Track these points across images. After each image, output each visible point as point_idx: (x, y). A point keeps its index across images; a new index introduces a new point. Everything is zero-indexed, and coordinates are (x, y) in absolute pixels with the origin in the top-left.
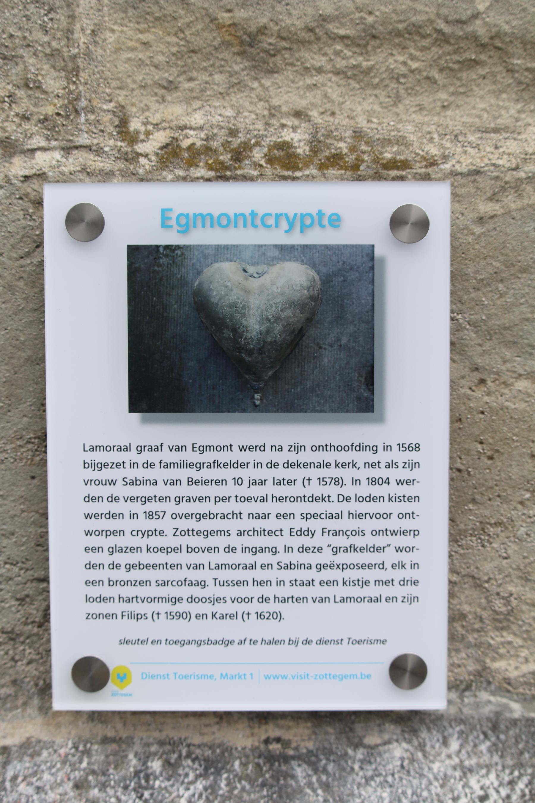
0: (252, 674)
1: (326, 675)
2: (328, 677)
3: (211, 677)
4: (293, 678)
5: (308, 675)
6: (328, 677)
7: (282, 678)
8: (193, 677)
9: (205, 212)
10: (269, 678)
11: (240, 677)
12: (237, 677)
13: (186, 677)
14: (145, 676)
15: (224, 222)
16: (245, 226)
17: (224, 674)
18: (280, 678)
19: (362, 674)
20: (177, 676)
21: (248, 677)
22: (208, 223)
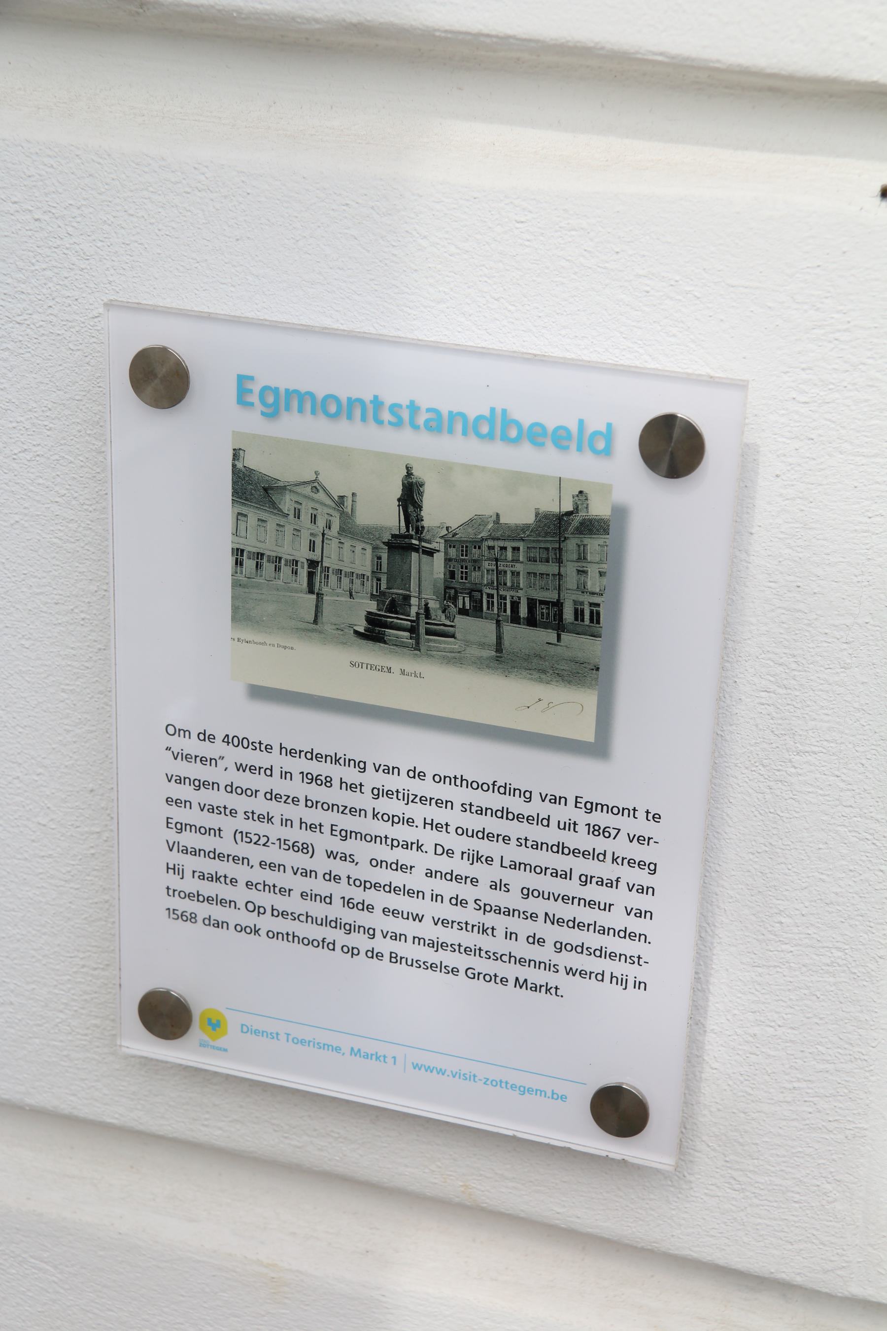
2: (504, 1085)
3: (337, 1049)
6: (504, 1085)
8: (311, 1044)
9: (303, 389)
10: (420, 1069)
11: (378, 1058)
13: (302, 1042)
14: (245, 1029)
15: (333, 409)
16: (364, 419)
17: (356, 1051)
19: (553, 1094)
20: (291, 1038)
21: (390, 1060)
22: (308, 406)
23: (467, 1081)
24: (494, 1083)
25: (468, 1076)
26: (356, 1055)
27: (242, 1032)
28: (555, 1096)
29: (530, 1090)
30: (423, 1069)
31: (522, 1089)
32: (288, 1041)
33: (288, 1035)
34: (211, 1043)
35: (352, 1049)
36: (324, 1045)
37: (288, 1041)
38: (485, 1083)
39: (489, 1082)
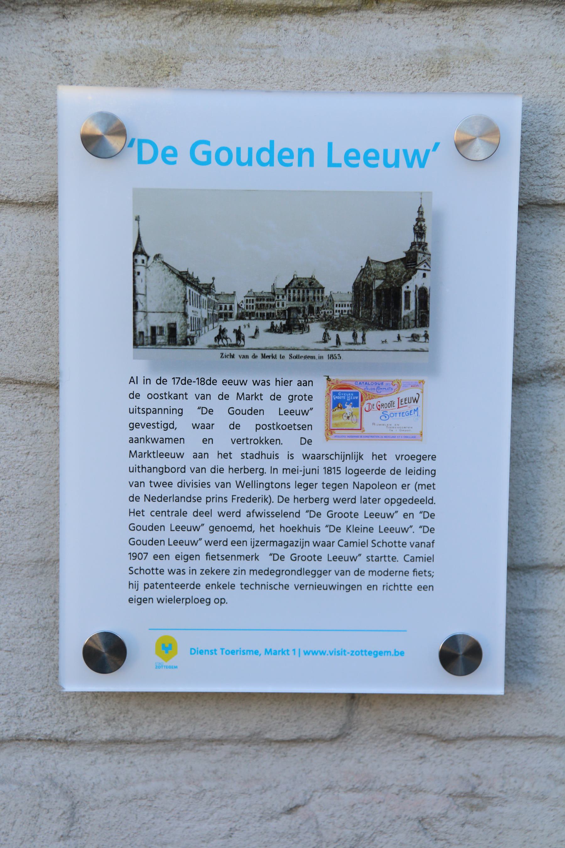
0: (294, 650)
2: (363, 653)
3: (256, 652)
4: (331, 654)
6: (363, 653)
7: (321, 654)
11: (283, 653)
12: (281, 653)
13: (233, 652)
17: (268, 650)
18: (319, 654)
19: (395, 652)
20: (224, 651)
21: (291, 652)
23: (340, 656)
24: (357, 653)
25: (340, 652)
26: (268, 654)
27: (191, 654)
28: (397, 654)
29: (381, 653)
30: (311, 653)
31: (375, 653)
33: (222, 649)
35: (266, 650)
36: (247, 651)
37: (222, 654)
38: (352, 655)
39: (354, 653)
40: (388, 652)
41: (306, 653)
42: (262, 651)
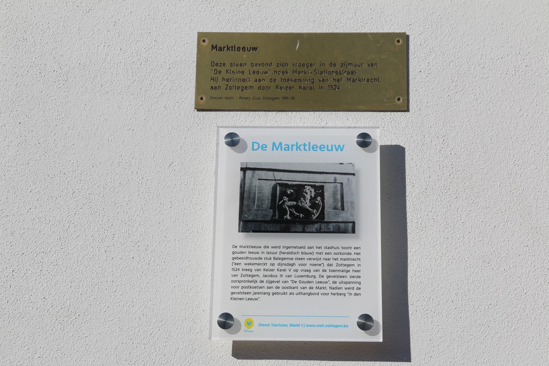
0: (302, 324)
1: (330, 325)
3: (286, 325)
4: (317, 326)
5: (323, 325)
6: (331, 326)
11: (297, 326)
13: (276, 325)
24: (328, 326)
29: (338, 326)
30: (309, 326)
32: (272, 326)
33: (272, 324)
34: (250, 330)
35: (290, 324)
37: (272, 326)
38: (326, 327)
40: (341, 326)
41: (307, 326)
42: (288, 325)
